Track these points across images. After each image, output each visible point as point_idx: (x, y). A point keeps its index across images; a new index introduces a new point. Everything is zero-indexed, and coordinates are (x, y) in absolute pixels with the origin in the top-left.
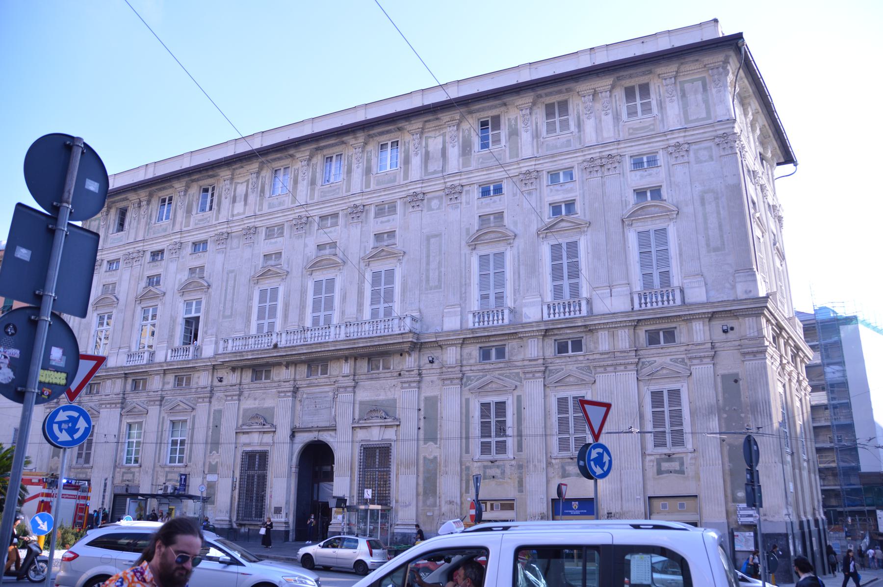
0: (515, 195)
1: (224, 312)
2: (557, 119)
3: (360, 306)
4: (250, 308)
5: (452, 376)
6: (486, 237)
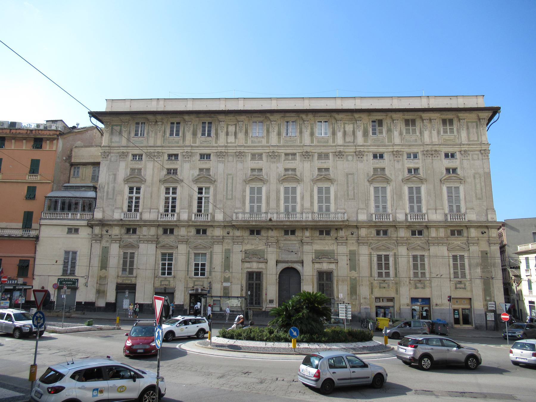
0: (390, 161)
1: (227, 196)
3: (312, 203)
4: (244, 197)
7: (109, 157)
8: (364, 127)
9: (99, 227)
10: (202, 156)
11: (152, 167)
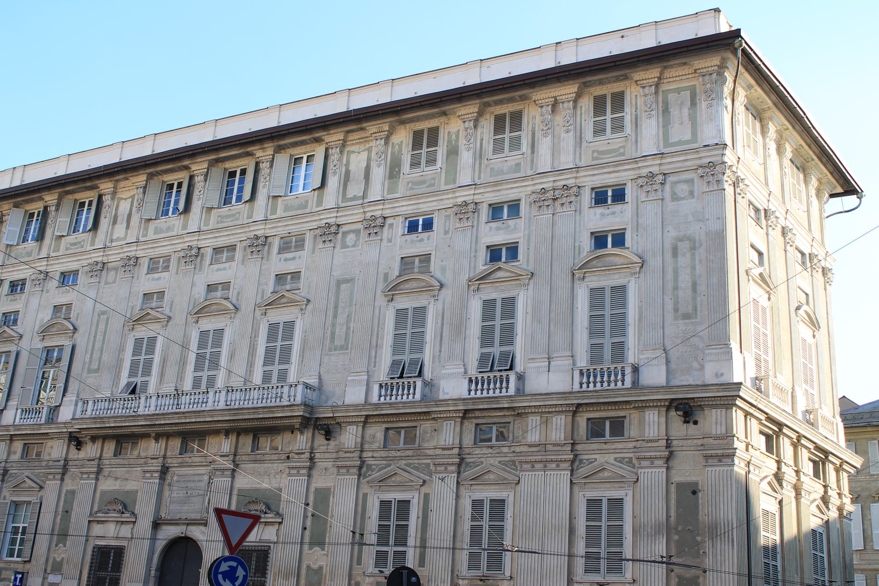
0: (446, 232)
2: (507, 135)
3: (251, 365)
5: (348, 463)
6: (407, 286)
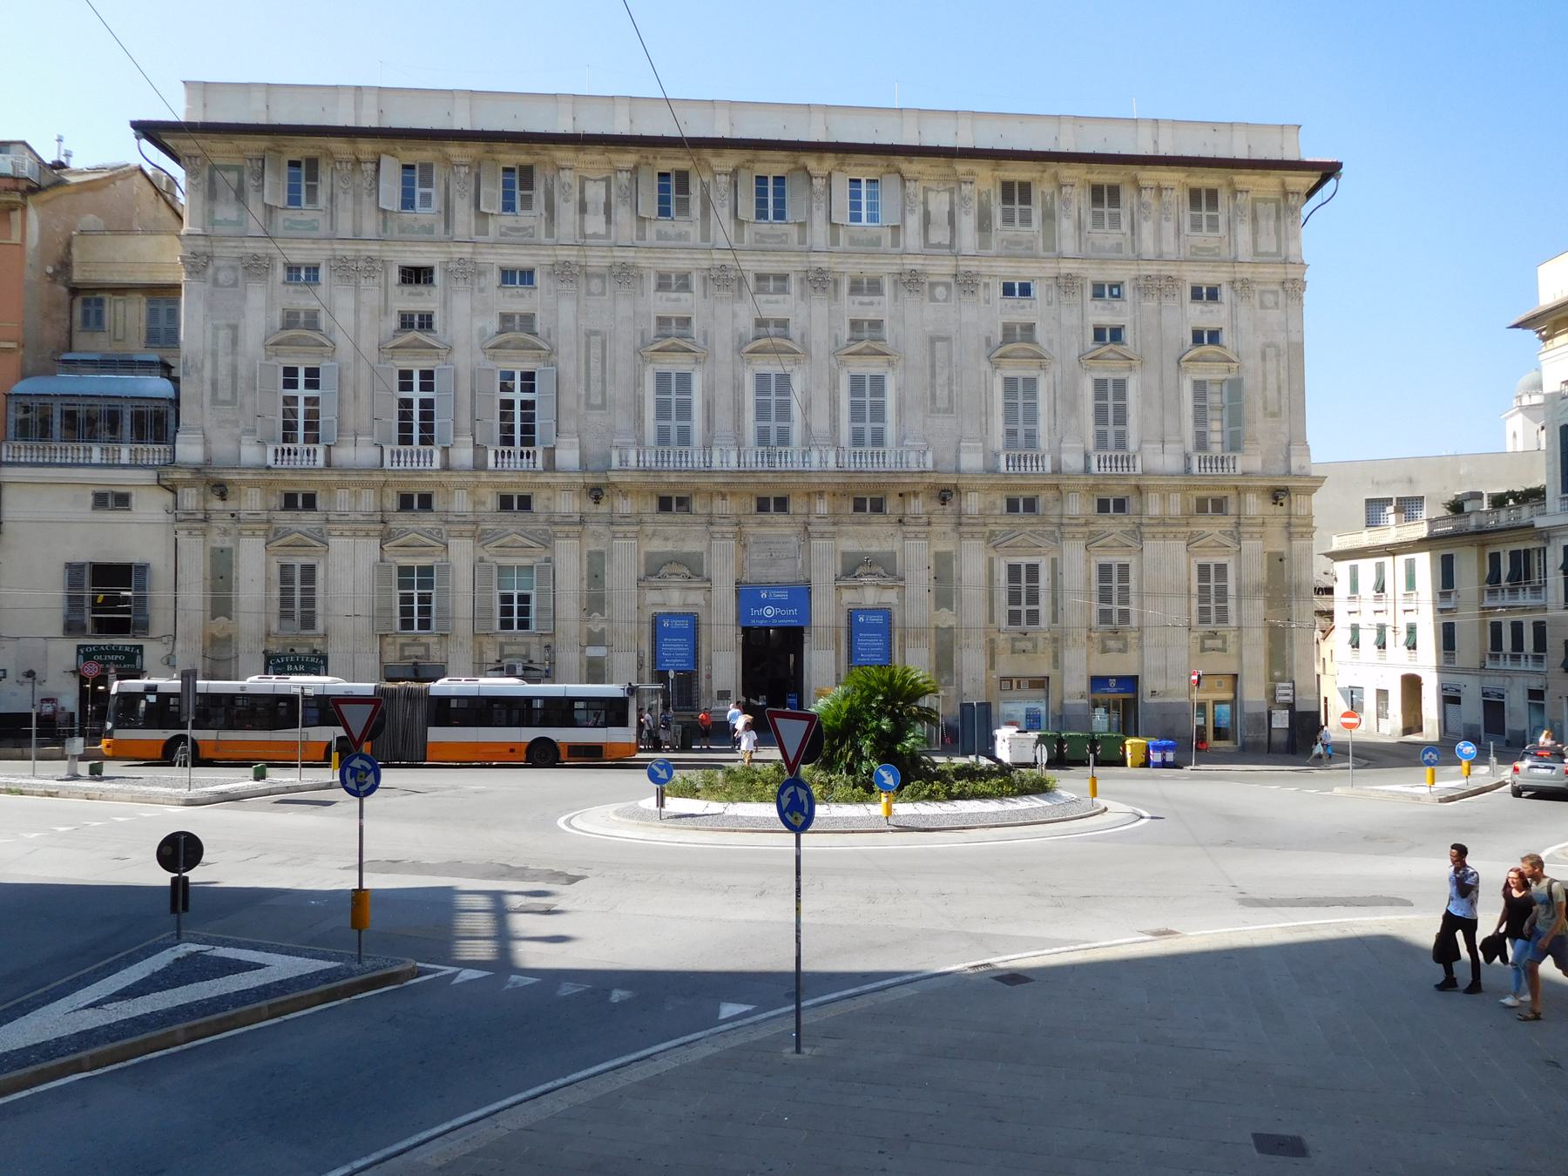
0: (1050, 303)
4: (639, 402)
7: (210, 271)
8: (980, 202)
9: (194, 491)
10: (508, 276)
11: (352, 305)
